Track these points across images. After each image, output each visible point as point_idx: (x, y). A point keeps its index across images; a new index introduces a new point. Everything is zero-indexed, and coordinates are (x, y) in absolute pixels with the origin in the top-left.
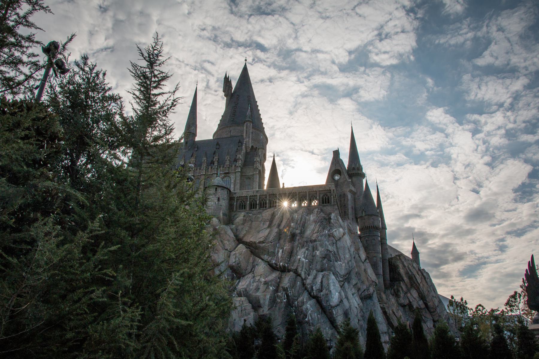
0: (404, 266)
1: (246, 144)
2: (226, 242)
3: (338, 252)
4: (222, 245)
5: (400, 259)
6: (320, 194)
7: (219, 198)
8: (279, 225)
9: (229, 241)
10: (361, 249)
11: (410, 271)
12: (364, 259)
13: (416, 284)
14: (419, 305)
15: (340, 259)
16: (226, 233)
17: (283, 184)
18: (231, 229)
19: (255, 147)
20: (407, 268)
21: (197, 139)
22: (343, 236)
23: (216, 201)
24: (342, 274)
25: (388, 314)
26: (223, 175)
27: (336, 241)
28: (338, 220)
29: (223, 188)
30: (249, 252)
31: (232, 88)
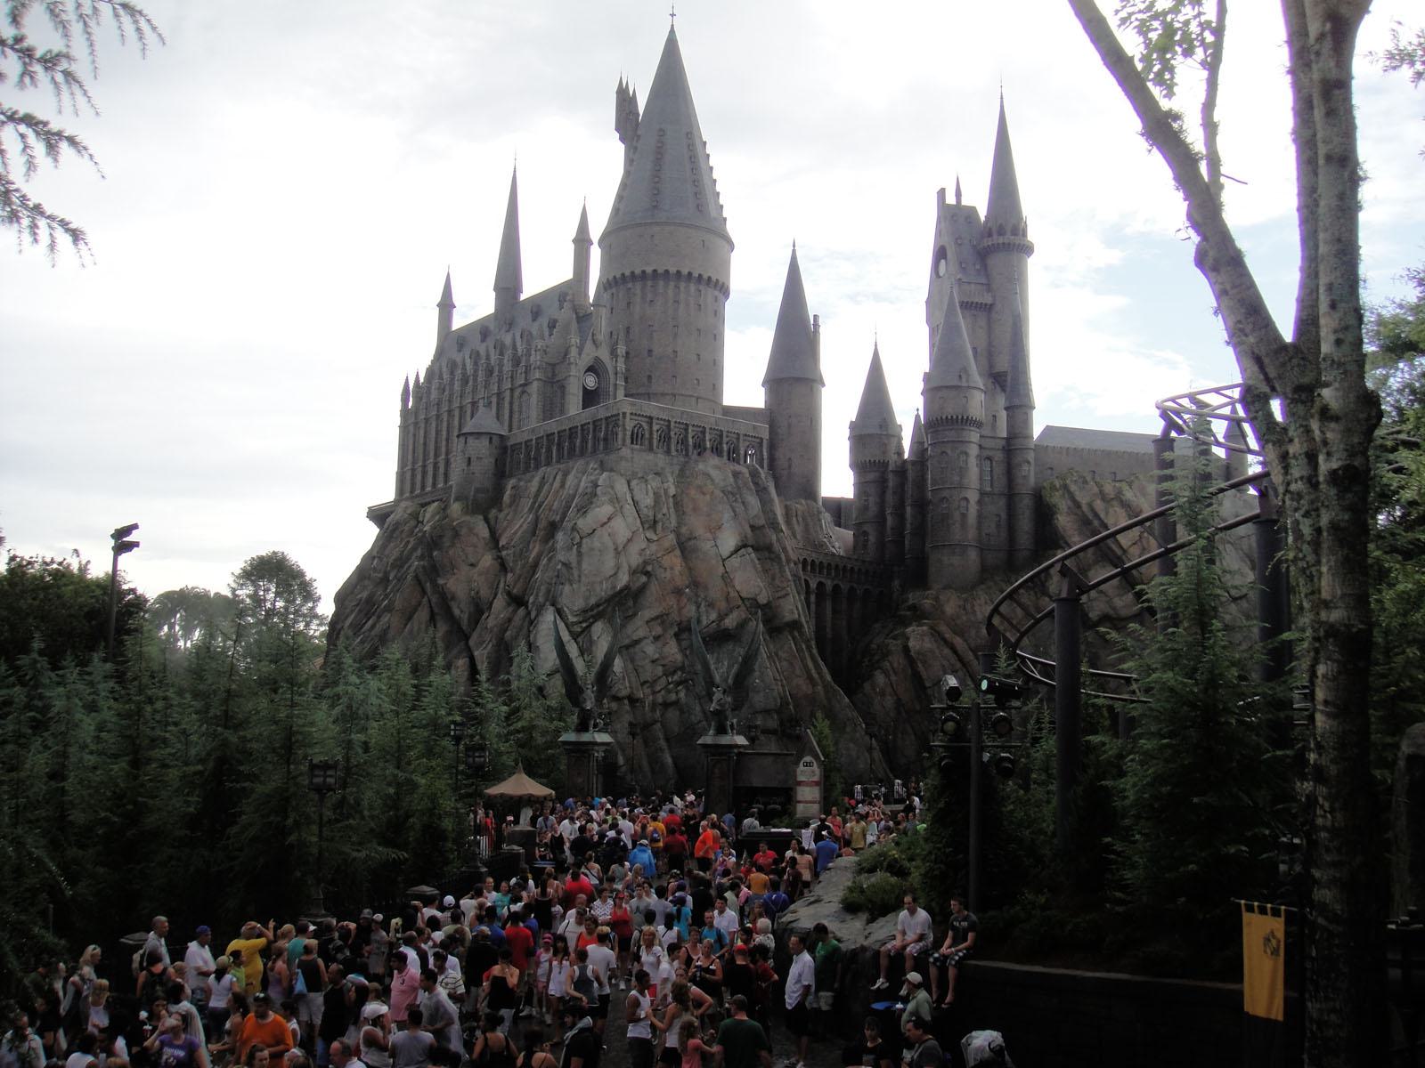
0: (1078, 506)
1: (572, 301)
2: (470, 550)
3: (579, 563)
4: (463, 558)
5: (1065, 487)
6: (607, 424)
7: (470, 459)
8: (540, 506)
9: (475, 546)
10: (726, 525)
11: (1096, 515)
12: (732, 549)
13: (1113, 551)
14: (1114, 609)
15: (580, 576)
16: (471, 530)
17: (815, 316)
18: (487, 520)
19: (660, 271)
20: (1085, 508)
21: (523, 297)
22: (605, 523)
23: (464, 466)
24: (576, 609)
25: (912, 653)
26: (519, 390)
27: (581, 538)
28: (612, 488)
29: (478, 435)
30: (498, 567)
31: (638, 115)
